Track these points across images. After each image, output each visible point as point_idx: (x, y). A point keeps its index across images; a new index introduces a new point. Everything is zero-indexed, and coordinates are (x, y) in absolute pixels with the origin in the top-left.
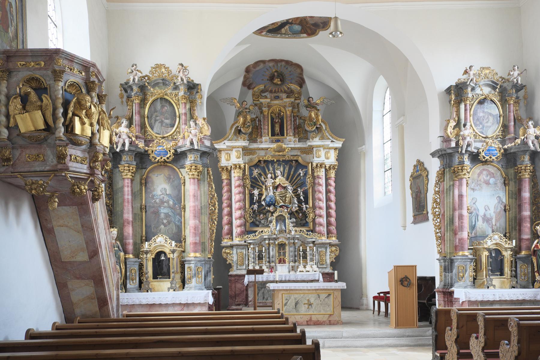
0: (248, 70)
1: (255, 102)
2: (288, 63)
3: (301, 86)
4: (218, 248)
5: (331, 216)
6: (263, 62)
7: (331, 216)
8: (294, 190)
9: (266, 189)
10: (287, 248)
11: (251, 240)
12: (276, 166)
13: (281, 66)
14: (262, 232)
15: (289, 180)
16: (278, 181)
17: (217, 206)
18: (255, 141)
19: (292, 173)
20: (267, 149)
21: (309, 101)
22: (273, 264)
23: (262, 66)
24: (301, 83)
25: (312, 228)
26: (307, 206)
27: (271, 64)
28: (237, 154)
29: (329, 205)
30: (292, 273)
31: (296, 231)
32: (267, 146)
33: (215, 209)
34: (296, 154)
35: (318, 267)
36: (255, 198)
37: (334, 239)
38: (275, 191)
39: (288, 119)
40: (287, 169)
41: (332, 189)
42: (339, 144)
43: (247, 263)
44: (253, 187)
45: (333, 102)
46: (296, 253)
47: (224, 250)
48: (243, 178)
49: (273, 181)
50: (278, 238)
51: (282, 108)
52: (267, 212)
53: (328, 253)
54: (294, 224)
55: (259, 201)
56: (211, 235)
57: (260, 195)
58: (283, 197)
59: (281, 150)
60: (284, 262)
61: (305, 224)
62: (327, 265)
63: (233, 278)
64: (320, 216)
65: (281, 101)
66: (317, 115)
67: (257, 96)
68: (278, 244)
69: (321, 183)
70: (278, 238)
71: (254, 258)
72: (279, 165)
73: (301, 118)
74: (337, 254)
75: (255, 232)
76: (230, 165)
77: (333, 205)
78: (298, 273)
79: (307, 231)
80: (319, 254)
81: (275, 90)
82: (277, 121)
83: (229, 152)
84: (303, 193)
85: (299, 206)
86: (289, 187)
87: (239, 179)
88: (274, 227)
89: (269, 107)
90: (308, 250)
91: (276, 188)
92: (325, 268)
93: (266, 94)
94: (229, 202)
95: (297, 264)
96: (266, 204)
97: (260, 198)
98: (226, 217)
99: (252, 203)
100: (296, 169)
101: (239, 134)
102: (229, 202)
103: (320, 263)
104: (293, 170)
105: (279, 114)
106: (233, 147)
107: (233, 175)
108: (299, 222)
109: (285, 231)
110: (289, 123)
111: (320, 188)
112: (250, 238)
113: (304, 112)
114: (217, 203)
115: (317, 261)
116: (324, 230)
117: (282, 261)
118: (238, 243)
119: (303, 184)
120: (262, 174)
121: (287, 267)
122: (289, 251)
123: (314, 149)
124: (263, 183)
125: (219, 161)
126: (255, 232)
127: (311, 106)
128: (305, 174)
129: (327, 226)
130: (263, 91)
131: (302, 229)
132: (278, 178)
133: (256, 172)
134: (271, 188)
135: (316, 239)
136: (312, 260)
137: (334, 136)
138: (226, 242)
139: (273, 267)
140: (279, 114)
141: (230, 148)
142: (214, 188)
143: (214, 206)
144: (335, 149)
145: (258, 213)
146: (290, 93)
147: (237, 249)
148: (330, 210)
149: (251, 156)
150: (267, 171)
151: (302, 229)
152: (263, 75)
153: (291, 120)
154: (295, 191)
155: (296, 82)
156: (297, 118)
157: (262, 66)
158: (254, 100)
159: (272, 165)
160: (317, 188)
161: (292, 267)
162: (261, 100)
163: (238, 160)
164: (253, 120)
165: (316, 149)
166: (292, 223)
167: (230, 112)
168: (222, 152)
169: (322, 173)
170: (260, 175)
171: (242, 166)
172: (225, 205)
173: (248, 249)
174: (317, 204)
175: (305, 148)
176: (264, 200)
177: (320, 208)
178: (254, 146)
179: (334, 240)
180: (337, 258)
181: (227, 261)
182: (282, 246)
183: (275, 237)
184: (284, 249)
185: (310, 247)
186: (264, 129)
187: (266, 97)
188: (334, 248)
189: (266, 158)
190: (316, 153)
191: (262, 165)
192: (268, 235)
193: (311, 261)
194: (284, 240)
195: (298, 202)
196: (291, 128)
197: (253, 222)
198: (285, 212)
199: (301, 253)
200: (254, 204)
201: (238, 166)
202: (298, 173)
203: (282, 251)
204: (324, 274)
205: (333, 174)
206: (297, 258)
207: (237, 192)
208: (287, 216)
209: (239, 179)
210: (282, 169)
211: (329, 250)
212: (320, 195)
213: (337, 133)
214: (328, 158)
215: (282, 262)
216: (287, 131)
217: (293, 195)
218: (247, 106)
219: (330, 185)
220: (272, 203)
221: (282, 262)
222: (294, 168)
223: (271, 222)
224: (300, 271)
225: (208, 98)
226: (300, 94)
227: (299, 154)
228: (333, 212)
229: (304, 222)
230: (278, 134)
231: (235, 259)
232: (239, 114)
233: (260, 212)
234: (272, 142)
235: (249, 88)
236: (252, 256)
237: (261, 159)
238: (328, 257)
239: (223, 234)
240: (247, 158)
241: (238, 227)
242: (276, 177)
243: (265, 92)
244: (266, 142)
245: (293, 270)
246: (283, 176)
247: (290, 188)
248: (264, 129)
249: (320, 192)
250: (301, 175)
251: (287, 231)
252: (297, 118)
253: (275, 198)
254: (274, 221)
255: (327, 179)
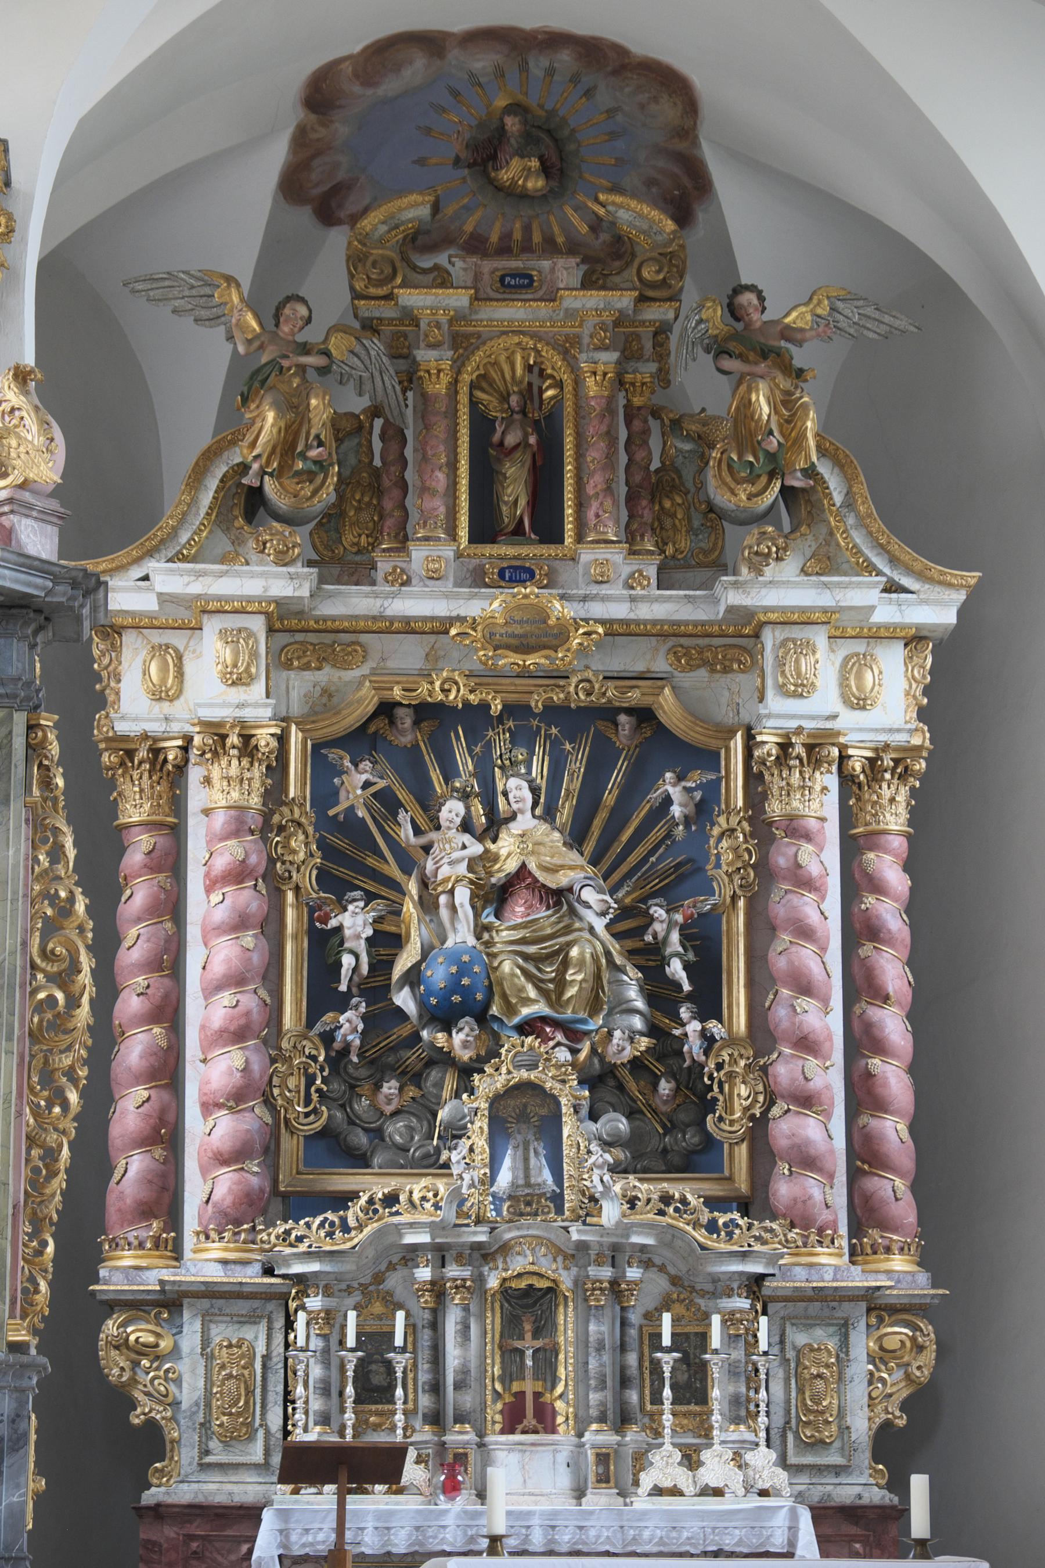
0: (321, 95)
1: (369, 309)
2: (597, 55)
3: (683, 216)
4: (77, 1310)
5: (880, 1106)
6: (431, 43)
7: (880, 1106)
8: (625, 912)
9: (428, 905)
10: (567, 1321)
11: (309, 1255)
12: (500, 743)
13: (550, 72)
14: (391, 1199)
15: (589, 847)
16: (507, 848)
17: (85, 977)
18: (356, 570)
19: (609, 798)
20: (440, 627)
21: (734, 311)
22: (460, 1436)
23: (417, 68)
24: (686, 192)
25: (743, 1184)
26: (713, 1025)
27: (482, 62)
28: (228, 655)
29: (869, 1027)
30: (599, 1500)
31: (632, 1202)
32: (440, 608)
33: (73, 1002)
34: (640, 667)
35: (783, 1462)
36: (347, 960)
37: (899, 1263)
38: (488, 917)
39: (594, 429)
40: (577, 766)
41: (890, 914)
42: (937, 609)
43: (275, 1420)
44: (336, 886)
45: (902, 323)
46: (632, 1359)
47: (111, 1327)
48: (268, 822)
49: (476, 849)
50: (506, 1249)
51: (547, 352)
52: (430, 1063)
53: (860, 1367)
54: (620, 1154)
55: (375, 987)
56: (36, 1184)
57: (386, 941)
58: (547, 960)
59: (536, 635)
60: (545, 1420)
61: (699, 1158)
62: (849, 1449)
63: (170, 1532)
64: (807, 1101)
65: (543, 309)
66: (788, 408)
67: (375, 272)
68: (505, 1292)
69: (814, 869)
70: (506, 1249)
71: (325, 1391)
72: (524, 738)
73: (676, 424)
74: (923, 1376)
75: (342, 1200)
76: (176, 727)
77: (893, 1024)
78: (641, 1502)
79: (713, 1203)
80: (795, 1364)
81: (506, 236)
82: (511, 440)
83: (177, 639)
84: (685, 938)
85: (653, 1030)
86: (589, 895)
87: (237, 830)
88: (478, 1169)
89: (462, 341)
90: (716, 1340)
91: (494, 896)
92: (838, 1470)
93: (441, 259)
94: (160, 984)
95: (633, 1436)
96: (422, 1003)
97: (382, 966)
98: (141, 1093)
99: (324, 995)
100: (638, 763)
101: (250, 516)
102: (160, 984)
103: (801, 1437)
104: (616, 777)
105: (530, 394)
106: (207, 607)
107: (196, 797)
108: (654, 1143)
109: (558, 1199)
110: (595, 454)
111: (807, 906)
112: (304, 1247)
113: (700, 385)
114: (86, 962)
115: (778, 1420)
116: (829, 1196)
117: (529, 1416)
118: (214, 1274)
119: (683, 877)
120: (402, 795)
121: (563, 1457)
122: (583, 1341)
123: (769, 638)
124: (407, 864)
125: (100, 702)
126: (342, 1200)
127: (749, 343)
128: (703, 810)
129: (854, 1175)
130: (419, 239)
131: (675, 1190)
132: (516, 828)
133: (357, 783)
134: (463, 895)
135: (773, 1259)
136: (741, 1411)
137: (907, 553)
138: (128, 1268)
139: (461, 1459)
140: (530, 394)
141: (184, 614)
142: (71, 853)
143: (64, 979)
144: (914, 639)
145: (360, 1072)
146: (606, 258)
147: (207, 1319)
148: (876, 1063)
149: (327, 675)
150: (435, 776)
151: (675, 1190)
152: (428, 131)
153: (611, 437)
154: (629, 923)
155: (650, 182)
156: (654, 425)
157: (417, 68)
158: (356, 295)
159: (472, 740)
160: (783, 902)
161: (603, 1459)
162: (412, 298)
163: (236, 694)
164: (348, 429)
165: (781, 633)
166: (607, 1145)
167: (191, 372)
168: (129, 639)
169: (820, 801)
170: (387, 803)
171: (265, 737)
172: (131, 1004)
173: (289, 1325)
174: (780, 1014)
175: (702, 631)
176: (413, 977)
177: (807, 1044)
178: (354, 602)
179: (898, 1271)
180: (922, 1402)
181: (133, 1405)
182: (529, 1306)
183: (481, 1235)
184: (545, 1326)
185: (730, 1319)
186: (424, 490)
187: (442, 279)
188: (897, 1333)
189: (430, 691)
190: (780, 664)
191: (406, 733)
192: (433, 1227)
193: (736, 1420)
194: (547, 1266)
195: (651, 999)
196: (609, 490)
197: (324, 1133)
198: (556, 1069)
199: (667, 1361)
200: (342, 1003)
201: (234, 739)
202: (655, 796)
203: (529, 1345)
204: (824, 1515)
205: (893, 813)
206: (633, 1396)
207: (221, 915)
208: (570, 1094)
209: (237, 830)
210: (539, 768)
211: (861, 1344)
212: (806, 956)
213: (924, 531)
214: (860, 703)
215: (530, 1420)
216: (580, 506)
217: (614, 947)
218: (313, 335)
219: (878, 888)
220: (469, 1002)
221: (530, 1420)
222: (622, 765)
223: (455, 1132)
224: (658, 1491)
225: (44, 266)
226: (673, 261)
227: (661, 665)
228: (894, 1078)
229: (691, 1138)
230: (518, 531)
231: (191, 1389)
232: (250, 382)
233: (378, 1067)
234: (478, 579)
235: (327, 213)
236: (316, 1371)
237: (397, 693)
238: (857, 1392)
239: (112, 1214)
240: (300, 685)
241: (223, 1159)
242: (495, 824)
243: (432, 248)
244: (434, 577)
245: (603, 1479)
246: (549, 815)
247: (595, 902)
248: (424, 490)
249: (805, 932)
250: (676, 810)
251: (570, 1198)
252: (654, 425)
253: (491, 970)
254: (480, 1125)
255: (854, 845)
